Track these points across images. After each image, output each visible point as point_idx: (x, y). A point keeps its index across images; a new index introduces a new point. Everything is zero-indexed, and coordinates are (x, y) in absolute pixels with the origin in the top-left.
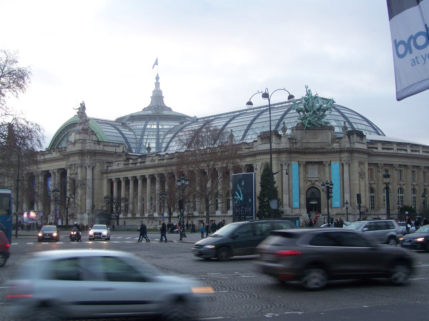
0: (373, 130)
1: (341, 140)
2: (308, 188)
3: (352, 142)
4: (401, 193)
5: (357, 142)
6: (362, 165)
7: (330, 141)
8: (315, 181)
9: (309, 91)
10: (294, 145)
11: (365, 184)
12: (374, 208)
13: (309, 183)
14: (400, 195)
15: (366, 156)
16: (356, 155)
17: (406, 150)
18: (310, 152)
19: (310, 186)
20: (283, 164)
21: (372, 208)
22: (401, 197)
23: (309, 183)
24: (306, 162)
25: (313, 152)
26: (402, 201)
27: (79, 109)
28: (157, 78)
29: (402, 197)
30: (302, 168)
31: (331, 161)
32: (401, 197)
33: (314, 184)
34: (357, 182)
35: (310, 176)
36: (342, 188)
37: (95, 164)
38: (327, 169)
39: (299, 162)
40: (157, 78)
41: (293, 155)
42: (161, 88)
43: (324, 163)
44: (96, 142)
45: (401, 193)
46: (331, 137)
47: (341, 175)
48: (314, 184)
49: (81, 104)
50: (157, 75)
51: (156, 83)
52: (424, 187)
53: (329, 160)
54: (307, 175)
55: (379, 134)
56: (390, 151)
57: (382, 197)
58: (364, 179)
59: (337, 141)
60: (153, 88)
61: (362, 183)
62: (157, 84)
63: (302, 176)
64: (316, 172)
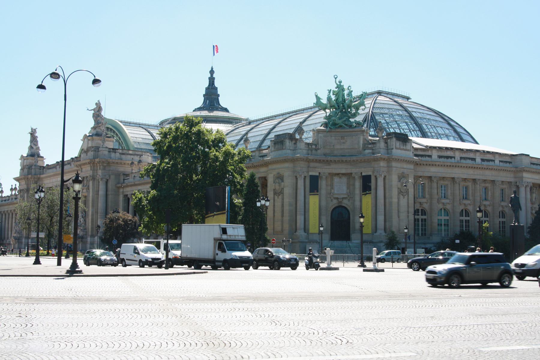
0: (454, 134)
2: (334, 207)
3: (389, 147)
4: (466, 216)
5: (396, 148)
8: (343, 198)
9: (340, 82)
10: (313, 151)
11: (408, 203)
12: (425, 235)
13: (335, 201)
14: (464, 218)
15: (412, 167)
17: (474, 159)
19: (336, 205)
20: (298, 176)
21: (422, 234)
22: (466, 220)
23: (335, 201)
24: (329, 174)
26: (468, 226)
27: (94, 110)
28: (212, 72)
29: (467, 222)
32: (466, 220)
33: (341, 202)
34: (395, 200)
35: (336, 192)
37: (110, 176)
40: (212, 72)
41: (312, 164)
42: (216, 84)
43: (353, 175)
44: (111, 150)
45: (466, 216)
46: (363, 141)
48: (341, 202)
49: (96, 104)
50: (212, 68)
51: (210, 78)
52: (501, 209)
54: (332, 191)
55: (462, 140)
56: (449, 160)
57: (436, 221)
58: (406, 197)
59: (370, 146)
60: (207, 84)
61: (403, 202)
62: (212, 80)
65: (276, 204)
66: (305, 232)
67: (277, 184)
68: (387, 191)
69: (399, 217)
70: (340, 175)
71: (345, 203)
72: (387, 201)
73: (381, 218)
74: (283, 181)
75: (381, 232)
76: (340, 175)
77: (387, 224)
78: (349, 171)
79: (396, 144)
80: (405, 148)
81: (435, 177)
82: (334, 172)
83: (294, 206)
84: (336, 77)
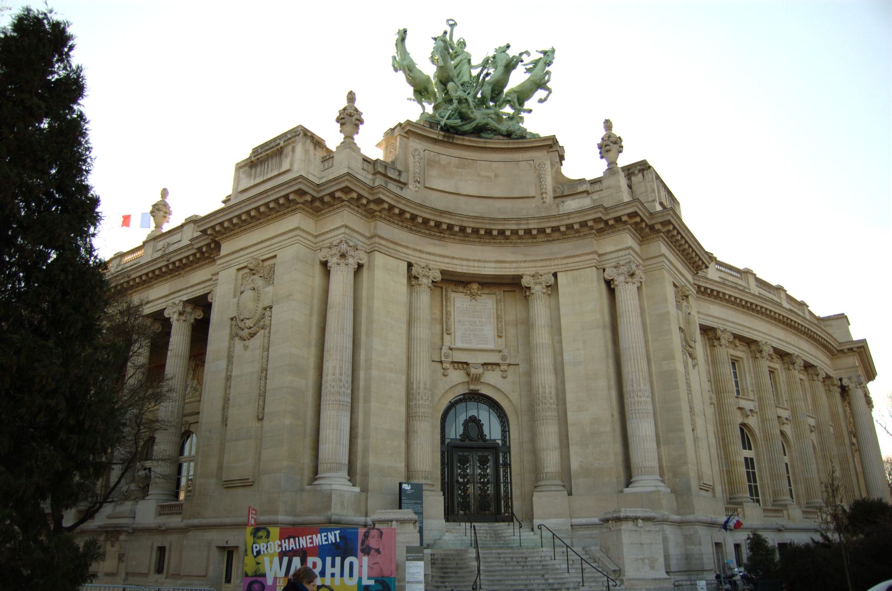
8: (485, 364)
23: (457, 376)
24: (443, 272)
25: (476, 231)
30: (424, 298)
31: (555, 275)
33: (477, 379)
34: (680, 367)
35: (459, 345)
38: (540, 309)
39: (410, 265)
41: (385, 229)
43: (525, 282)
48: (477, 379)
63: (424, 332)
64: (489, 331)
65: (235, 372)
67: (249, 294)
71: (493, 383)
73: (643, 430)
74: (269, 278)
76: (475, 286)
81: (724, 331)
83: (311, 374)
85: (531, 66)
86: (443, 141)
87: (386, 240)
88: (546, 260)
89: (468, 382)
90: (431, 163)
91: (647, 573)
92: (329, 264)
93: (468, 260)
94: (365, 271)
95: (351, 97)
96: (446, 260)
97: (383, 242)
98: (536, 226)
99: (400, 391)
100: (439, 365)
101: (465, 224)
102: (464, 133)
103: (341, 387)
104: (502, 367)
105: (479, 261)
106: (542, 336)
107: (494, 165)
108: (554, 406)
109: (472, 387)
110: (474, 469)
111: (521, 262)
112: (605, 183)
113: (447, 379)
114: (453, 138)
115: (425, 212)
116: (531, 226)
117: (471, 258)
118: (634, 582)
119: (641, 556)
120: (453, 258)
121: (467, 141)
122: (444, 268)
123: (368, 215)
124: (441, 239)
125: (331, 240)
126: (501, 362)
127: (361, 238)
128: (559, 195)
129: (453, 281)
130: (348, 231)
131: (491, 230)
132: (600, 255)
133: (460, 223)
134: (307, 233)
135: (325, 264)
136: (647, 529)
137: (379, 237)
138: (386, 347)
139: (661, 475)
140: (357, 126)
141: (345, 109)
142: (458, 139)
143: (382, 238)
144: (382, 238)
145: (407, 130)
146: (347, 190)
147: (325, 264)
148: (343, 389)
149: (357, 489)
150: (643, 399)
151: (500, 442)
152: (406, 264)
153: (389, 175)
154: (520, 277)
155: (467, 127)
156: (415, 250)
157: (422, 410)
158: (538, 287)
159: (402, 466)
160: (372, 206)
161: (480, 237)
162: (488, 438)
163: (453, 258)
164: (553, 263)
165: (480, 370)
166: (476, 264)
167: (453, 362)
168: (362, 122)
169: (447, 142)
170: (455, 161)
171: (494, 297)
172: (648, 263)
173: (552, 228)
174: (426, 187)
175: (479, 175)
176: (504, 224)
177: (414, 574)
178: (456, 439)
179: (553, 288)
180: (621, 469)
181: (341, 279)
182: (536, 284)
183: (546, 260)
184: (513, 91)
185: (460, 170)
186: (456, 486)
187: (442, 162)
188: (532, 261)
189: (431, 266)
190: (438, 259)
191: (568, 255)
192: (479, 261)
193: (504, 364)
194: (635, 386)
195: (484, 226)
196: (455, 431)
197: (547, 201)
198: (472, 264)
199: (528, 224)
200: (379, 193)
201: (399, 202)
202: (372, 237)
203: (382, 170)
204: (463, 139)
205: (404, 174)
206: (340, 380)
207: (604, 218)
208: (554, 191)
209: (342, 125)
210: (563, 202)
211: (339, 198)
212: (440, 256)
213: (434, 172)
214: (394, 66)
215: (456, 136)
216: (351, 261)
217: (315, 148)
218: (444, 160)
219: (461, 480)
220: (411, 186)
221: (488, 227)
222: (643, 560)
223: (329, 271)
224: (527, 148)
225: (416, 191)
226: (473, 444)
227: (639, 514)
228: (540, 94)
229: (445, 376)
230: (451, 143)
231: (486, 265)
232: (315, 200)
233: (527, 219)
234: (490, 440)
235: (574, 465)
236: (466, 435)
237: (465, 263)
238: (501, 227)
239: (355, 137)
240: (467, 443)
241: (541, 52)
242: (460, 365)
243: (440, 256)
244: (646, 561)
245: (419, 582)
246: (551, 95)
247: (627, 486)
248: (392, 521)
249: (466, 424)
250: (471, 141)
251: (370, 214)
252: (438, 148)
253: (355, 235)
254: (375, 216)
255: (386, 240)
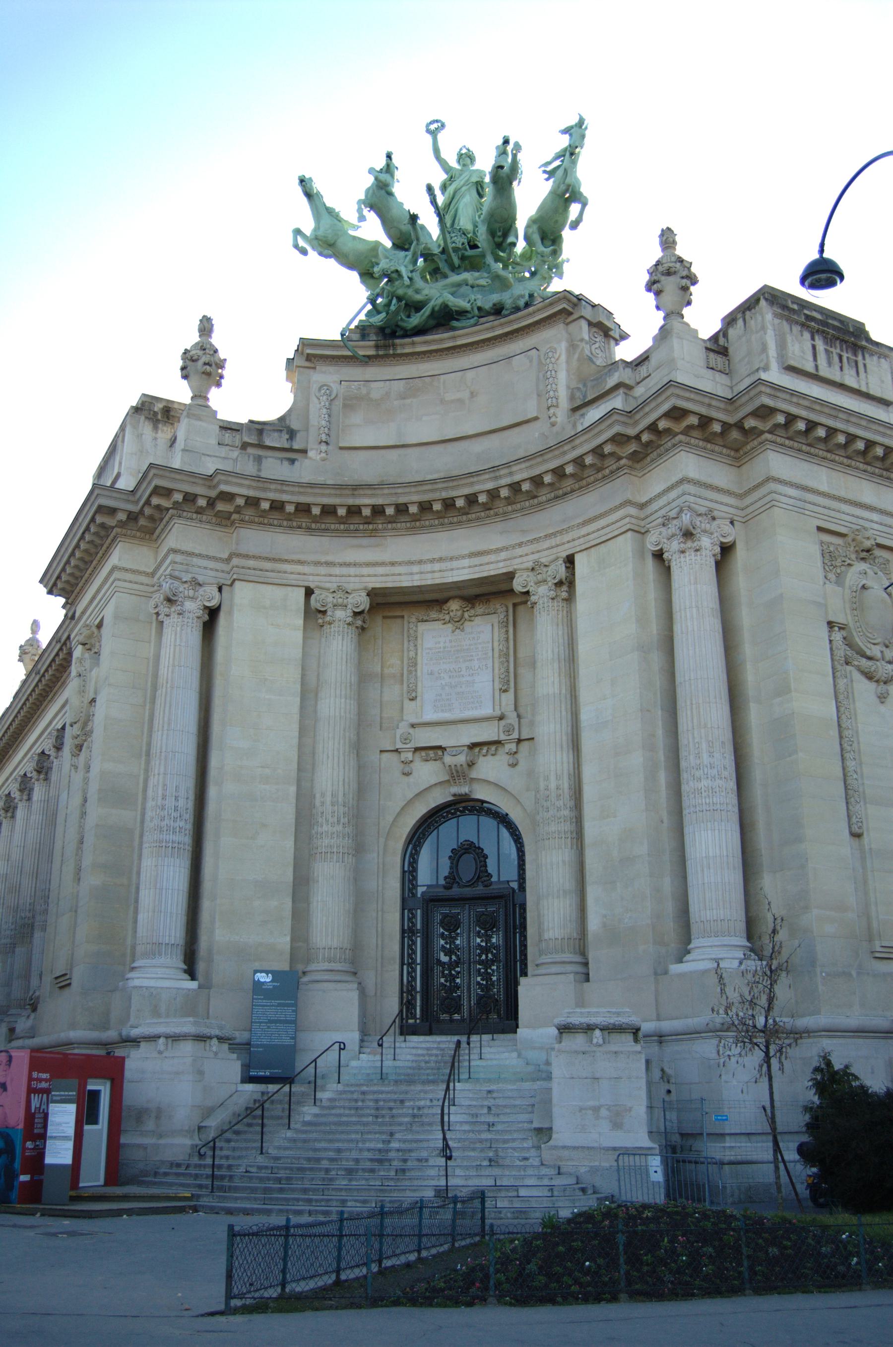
1: (643, 370)
2: (421, 810)
5: (792, 369)
6: (863, 566)
7: (564, 403)
8: (473, 746)
9: (466, 157)
16: (777, 462)
18: (402, 509)
23: (427, 773)
24: (372, 593)
25: (425, 507)
30: (339, 646)
31: (570, 561)
36: (662, 777)
38: (545, 629)
39: (309, 592)
41: (255, 539)
43: (518, 585)
47: (657, 659)
48: (457, 775)
53: (550, 554)
63: (334, 706)
66: (191, 972)
68: (748, 650)
69: (857, 835)
70: (454, 606)
71: (493, 780)
72: (755, 716)
75: (718, 949)
77: (770, 885)
78: (493, 567)
79: (782, 346)
80: (850, 381)
82: (406, 582)
84: (432, 127)
85: (557, 163)
86: (376, 357)
87: (255, 557)
88: (554, 534)
89: (448, 781)
90: (350, 404)
91: (604, 1135)
92: (665, 556)
93: (420, 562)
94: (222, 620)
95: (667, 239)
96: (380, 570)
97: (251, 563)
98: (525, 475)
99: (288, 811)
100: (394, 757)
101: (402, 500)
102: (420, 331)
103: (175, 820)
104: (403, 756)
105: (441, 560)
106: (547, 682)
107: (470, 374)
108: (566, 813)
109: (455, 790)
110: (469, 939)
111: (513, 547)
112: (653, 361)
113: (411, 779)
114: (394, 346)
115: (323, 495)
116: (517, 478)
117: (425, 558)
118: (566, 1153)
119: (591, 1103)
120: (393, 564)
121: (421, 344)
122: (378, 585)
123: (224, 522)
124: (373, 534)
125: (662, 512)
126: (503, 737)
127: (212, 564)
128: (579, 403)
129: (388, 605)
130: (179, 558)
131: (453, 499)
132: (642, 506)
133: (393, 500)
134: (134, 571)
135: (659, 556)
136: (613, 1048)
137: (239, 555)
138: (258, 742)
139: (749, 938)
140: (685, 289)
141: (658, 263)
142: (405, 346)
143: (247, 557)
144: (247, 557)
145: (310, 356)
146: (676, 414)
147: (659, 556)
148: (166, 822)
149: (194, 985)
150: (704, 783)
151: (515, 885)
152: (303, 591)
153: (268, 442)
154: (510, 576)
155: (415, 320)
156: (317, 563)
157: (326, 841)
158: (543, 590)
159: (284, 941)
160: (221, 506)
161: (463, 512)
162: (494, 879)
163: (393, 564)
164: (566, 538)
165: (462, 759)
166: (437, 566)
167: (417, 749)
168: (694, 280)
169: (382, 357)
170: (400, 386)
171: (494, 619)
172: (748, 500)
173: (324, 506)
174: (341, 448)
175: (442, 401)
176: (472, 484)
177: (60, 1124)
178: (437, 886)
179: (567, 584)
180: (670, 925)
181: (693, 576)
182: (538, 583)
183: (554, 534)
184: (533, 221)
185: (408, 401)
186: (438, 969)
187: (375, 395)
188: (531, 542)
189: (350, 587)
190: (366, 571)
191: (586, 517)
192: (441, 560)
193: (510, 741)
194: (705, 756)
195: (437, 495)
196: (429, 872)
197: (559, 420)
198: (428, 567)
199: (511, 474)
200: (219, 483)
201: (265, 490)
202: (228, 560)
203: (252, 439)
204: (413, 343)
205: (299, 436)
206: (163, 808)
207: (632, 432)
208: (572, 398)
209: (658, 294)
210: (583, 415)
211: (668, 431)
212: (368, 565)
213: (357, 418)
214: (296, 246)
215: (398, 341)
216: (705, 542)
217: (155, 428)
218: (377, 390)
219: (444, 959)
220: (311, 454)
221: (444, 495)
222: (596, 1109)
223: (669, 568)
224: (528, 327)
225: (323, 460)
226: (467, 891)
227: (593, 1020)
228: (574, 209)
229: (407, 774)
230: (395, 356)
231: (455, 564)
232: (219, 506)
233: (507, 465)
234: (499, 882)
235: (594, 924)
236: (452, 879)
237: (415, 569)
238: (467, 491)
239: (686, 311)
240: (456, 891)
241: (566, 131)
242: (431, 753)
243: (368, 565)
244: (604, 1112)
245: (66, 1138)
246: (587, 207)
247: (680, 961)
248: (210, 1038)
249: (457, 855)
250: (425, 342)
251: (225, 520)
252: (371, 372)
253: (195, 561)
254: (233, 523)
255: (255, 557)
